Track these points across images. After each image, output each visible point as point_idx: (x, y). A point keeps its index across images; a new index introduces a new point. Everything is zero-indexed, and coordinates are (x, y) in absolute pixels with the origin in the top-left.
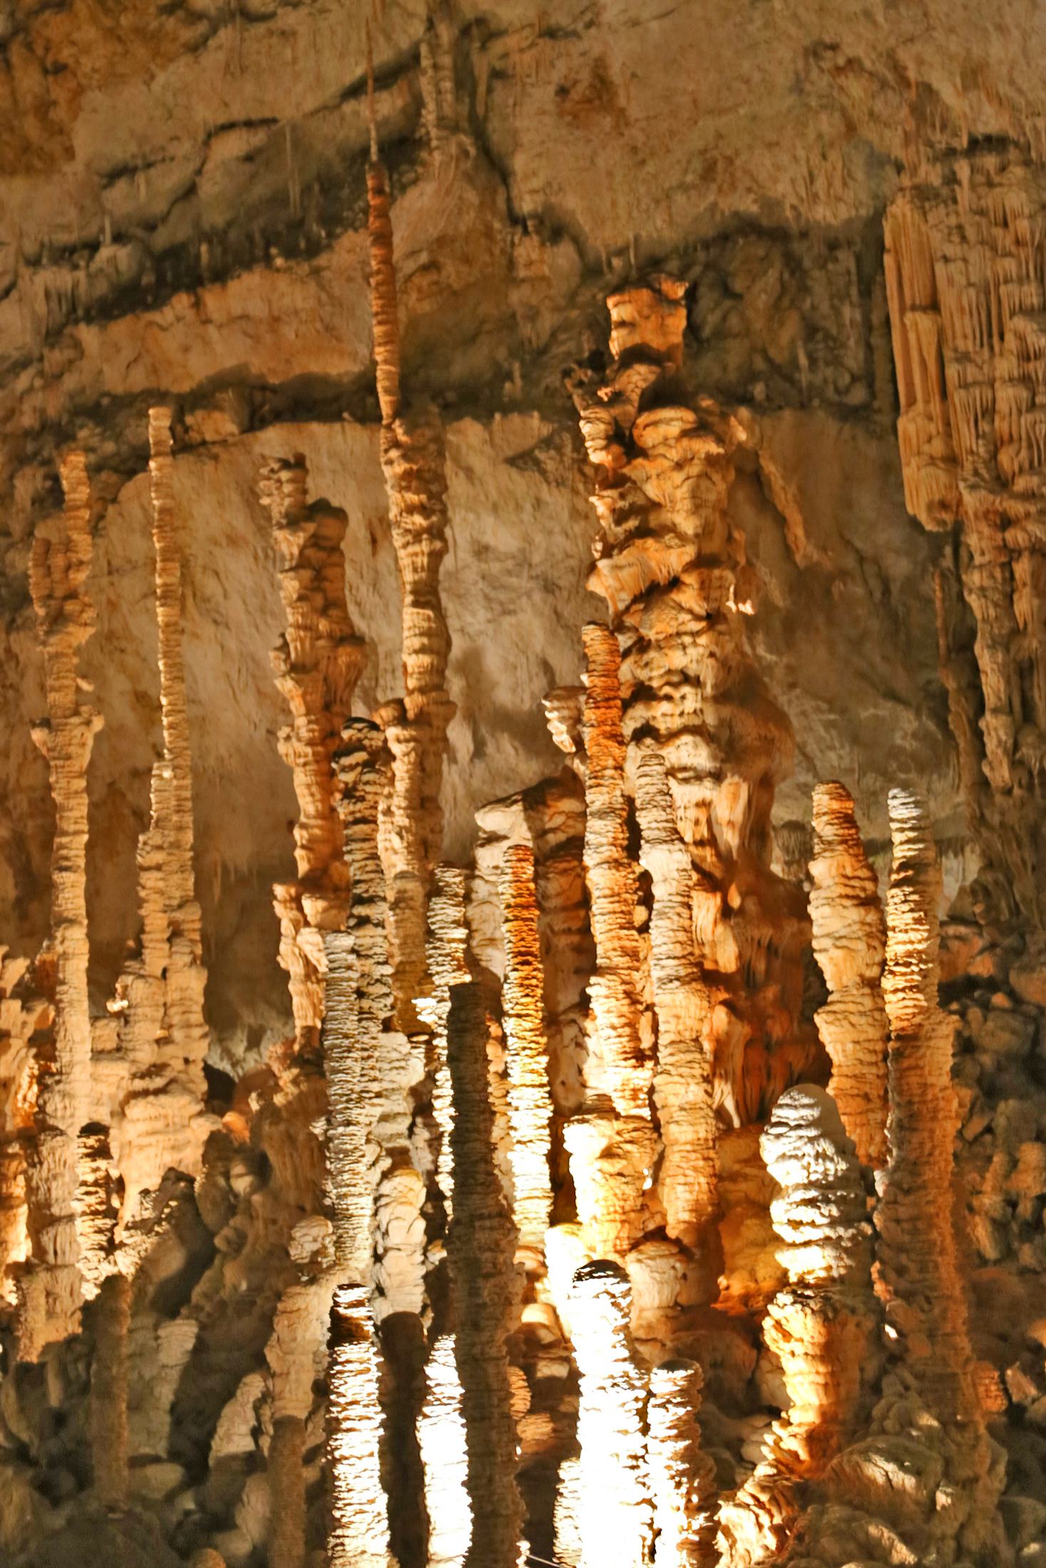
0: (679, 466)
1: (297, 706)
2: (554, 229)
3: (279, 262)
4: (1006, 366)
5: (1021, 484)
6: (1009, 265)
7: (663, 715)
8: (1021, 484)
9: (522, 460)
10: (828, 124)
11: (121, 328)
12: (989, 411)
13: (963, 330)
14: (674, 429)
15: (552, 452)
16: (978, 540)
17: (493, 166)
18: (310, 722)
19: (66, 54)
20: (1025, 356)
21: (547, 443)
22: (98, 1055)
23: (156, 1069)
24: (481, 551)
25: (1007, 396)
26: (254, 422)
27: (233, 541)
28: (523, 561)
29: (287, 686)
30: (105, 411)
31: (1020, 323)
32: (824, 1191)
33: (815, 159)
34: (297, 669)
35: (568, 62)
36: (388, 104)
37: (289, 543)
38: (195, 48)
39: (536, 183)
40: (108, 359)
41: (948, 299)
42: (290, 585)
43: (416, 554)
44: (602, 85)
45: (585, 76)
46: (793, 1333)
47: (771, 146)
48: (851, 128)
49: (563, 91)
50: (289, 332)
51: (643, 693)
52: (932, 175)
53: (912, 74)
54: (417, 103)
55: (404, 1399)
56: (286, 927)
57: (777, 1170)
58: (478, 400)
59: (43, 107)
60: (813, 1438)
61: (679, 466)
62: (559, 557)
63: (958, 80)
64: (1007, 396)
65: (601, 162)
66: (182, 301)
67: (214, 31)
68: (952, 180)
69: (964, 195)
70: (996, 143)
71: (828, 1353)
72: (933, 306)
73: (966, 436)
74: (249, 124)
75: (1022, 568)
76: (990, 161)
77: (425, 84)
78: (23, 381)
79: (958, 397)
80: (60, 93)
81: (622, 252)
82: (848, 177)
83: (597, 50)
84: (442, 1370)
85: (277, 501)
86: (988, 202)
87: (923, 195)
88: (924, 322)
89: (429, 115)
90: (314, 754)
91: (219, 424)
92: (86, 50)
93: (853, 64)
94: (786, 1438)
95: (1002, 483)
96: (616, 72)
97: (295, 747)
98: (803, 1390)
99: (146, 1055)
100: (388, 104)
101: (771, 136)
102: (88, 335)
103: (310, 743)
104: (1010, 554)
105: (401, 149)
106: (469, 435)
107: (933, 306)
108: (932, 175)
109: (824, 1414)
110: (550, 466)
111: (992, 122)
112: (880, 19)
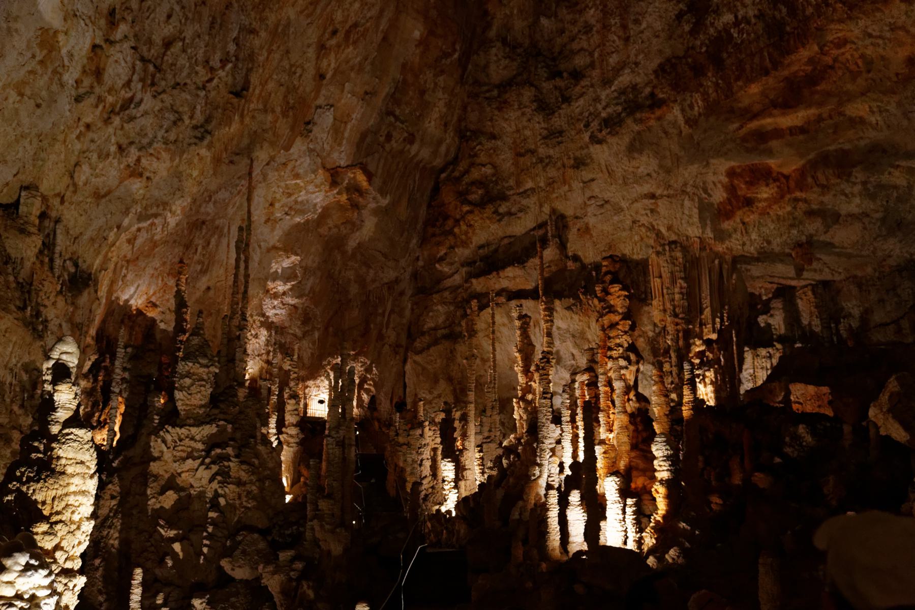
0: (618, 297)
1: (519, 359)
2: (576, 258)
4: (677, 290)
5: (680, 316)
6: (678, 268)
7: (614, 353)
8: (680, 316)
9: (568, 308)
10: (637, 238)
11: (481, 279)
12: (673, 300)
13: (667, 282)
14: (617, 289)
16: (670, 328)
17: (563, 246)
19: (472, 222)
20: (681, 288)
21: (574, 305)
22: (476, 433)
23: (488, 437)
24: (559, 328)
25: (677, 296)
26: (509, 299)
27: (504, 325)
28: (568, 331)
29: (517, 355)
30: (479, 296)
31: (680, 281)
32: (668, 458)
34: (519, 351)
35: (580, 224)
36: (541, 232)
37: (517, 323)
38: (499, 221)
40: (478, 285)
41: (664, 275)
42: (518, 332)
46: (660, 493)
48: (642, 239)
49: (579, 230)
50: (518, 280)
51: (610, 349)
52: (660, 249)
54: (547, 232)
55: (564, 503)
56: (516, 408)
57: (656, 453)
58: (560, 296)
59: (466, 233)
60: (664, 517)
61: (618, 297)
64: (677, 296)
66: (495, 273)
67: (503, 217)
68: (664, 250)
69: (667, 253)
70: (674, 242)
71: (668, 497)
72: (660, 277)
73: (668, 305)
74: (510, 237)
75: (681, 335)
76: (673, 246)
77: (549, 228)
78: (460, 290)
79: (666, 297)
80: (470, 231)
81: (591, 264)
82: (641, 249)
84: (575, 497)
85: (515, 314)
86: (673, 254)
87: (658, 253)
88: (658, 280)
89: (549, 234)
91: (502, 300)
92: (476, 221)
93: (643, 225)
94: (658, 517)
95: (676, 315)
96: (591, 226)
97: (518, 369)
98: (662, 505)
99: (486, 434)
100: (541, 232)
102: (474, 281)
104: (678, 331)
105: (544, 242)
106: (557, 303)
107: (660, 277)
108: (660, 249)
109: (667, 511)
111: (674, 237)
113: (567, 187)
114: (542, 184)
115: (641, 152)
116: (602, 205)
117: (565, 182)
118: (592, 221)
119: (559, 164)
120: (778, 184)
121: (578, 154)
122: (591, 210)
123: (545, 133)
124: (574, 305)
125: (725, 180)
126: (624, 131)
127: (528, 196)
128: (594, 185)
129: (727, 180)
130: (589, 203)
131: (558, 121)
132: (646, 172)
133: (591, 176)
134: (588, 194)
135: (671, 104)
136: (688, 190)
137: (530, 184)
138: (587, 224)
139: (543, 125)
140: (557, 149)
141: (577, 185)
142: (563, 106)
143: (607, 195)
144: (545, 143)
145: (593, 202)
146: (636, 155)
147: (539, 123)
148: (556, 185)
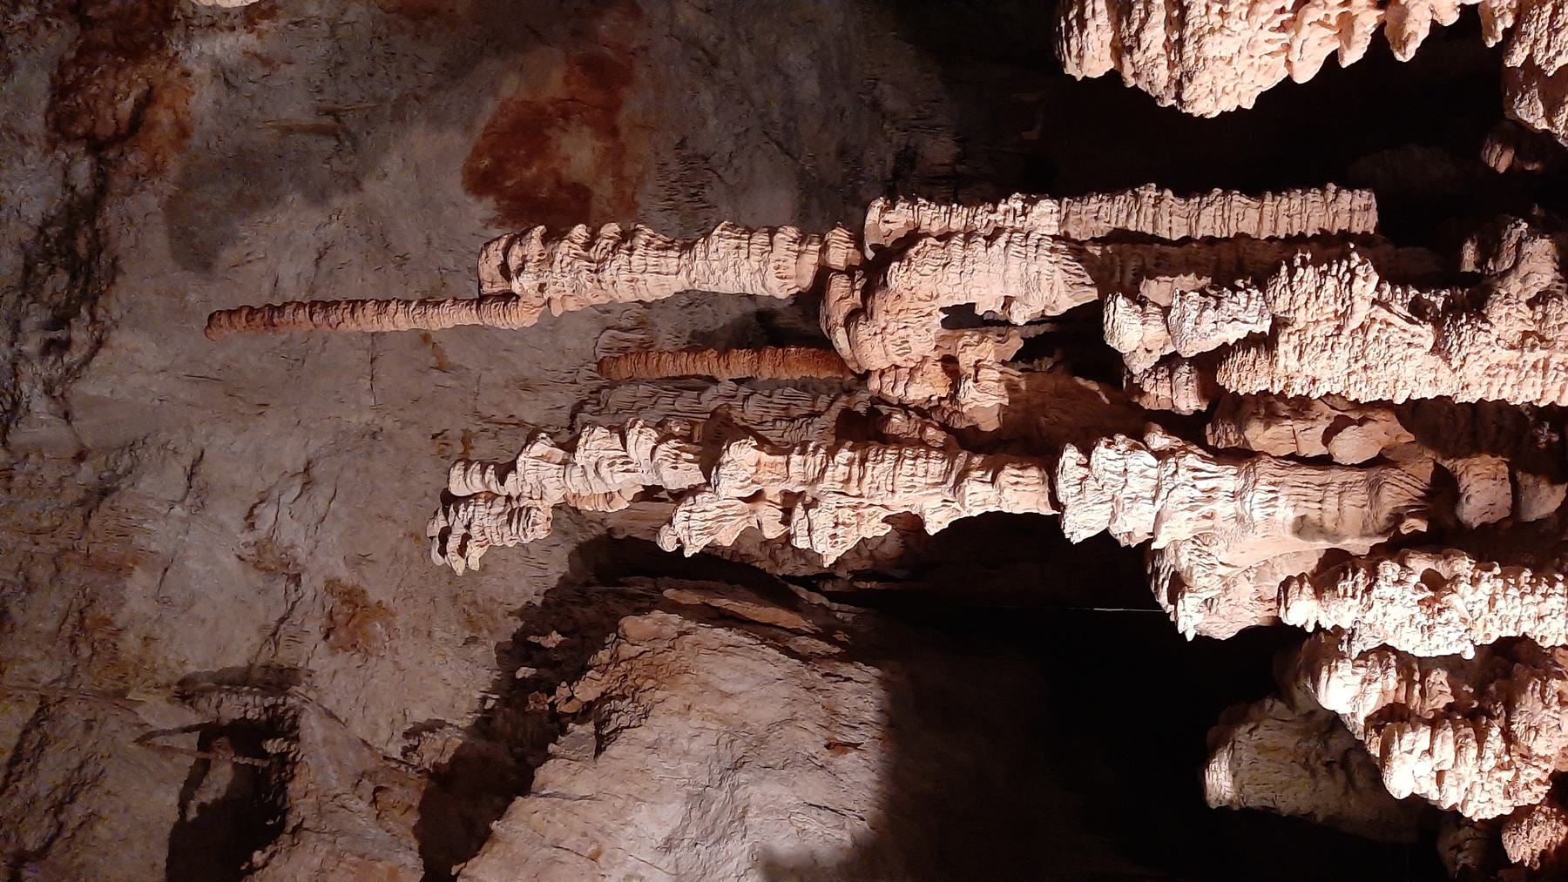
3: (258, 857)
15: (614, 716)
39: (384, 734)
43: (648, 244)
44: (352, 597)
45: (330, 602)
53: (500, 416)
62: (714, 751)
63: (524, 395)
65: (405, 663)
83: (319, 583)
90: (852, 449)
96: (346, 576)
110: (624, 721)
113: (139, 583)
114: (48, 672)
117: (119, 570)
118: (327, 562)
119: (41, 573)
121: (71, 494)
125: (484, 208)
126: (126, 243)
127: (41, 746)
128: (214, 470)
129: (490, 201)
130: (264, 527)
132: (306, 264)
133: (176, 472)
134: (230, 515)
135: (174, 75)
136: (449, 262)
138: (331, 585)
141: (159, 535)
143: (291, 454)
145: (267, 514)
146: (228, 255)
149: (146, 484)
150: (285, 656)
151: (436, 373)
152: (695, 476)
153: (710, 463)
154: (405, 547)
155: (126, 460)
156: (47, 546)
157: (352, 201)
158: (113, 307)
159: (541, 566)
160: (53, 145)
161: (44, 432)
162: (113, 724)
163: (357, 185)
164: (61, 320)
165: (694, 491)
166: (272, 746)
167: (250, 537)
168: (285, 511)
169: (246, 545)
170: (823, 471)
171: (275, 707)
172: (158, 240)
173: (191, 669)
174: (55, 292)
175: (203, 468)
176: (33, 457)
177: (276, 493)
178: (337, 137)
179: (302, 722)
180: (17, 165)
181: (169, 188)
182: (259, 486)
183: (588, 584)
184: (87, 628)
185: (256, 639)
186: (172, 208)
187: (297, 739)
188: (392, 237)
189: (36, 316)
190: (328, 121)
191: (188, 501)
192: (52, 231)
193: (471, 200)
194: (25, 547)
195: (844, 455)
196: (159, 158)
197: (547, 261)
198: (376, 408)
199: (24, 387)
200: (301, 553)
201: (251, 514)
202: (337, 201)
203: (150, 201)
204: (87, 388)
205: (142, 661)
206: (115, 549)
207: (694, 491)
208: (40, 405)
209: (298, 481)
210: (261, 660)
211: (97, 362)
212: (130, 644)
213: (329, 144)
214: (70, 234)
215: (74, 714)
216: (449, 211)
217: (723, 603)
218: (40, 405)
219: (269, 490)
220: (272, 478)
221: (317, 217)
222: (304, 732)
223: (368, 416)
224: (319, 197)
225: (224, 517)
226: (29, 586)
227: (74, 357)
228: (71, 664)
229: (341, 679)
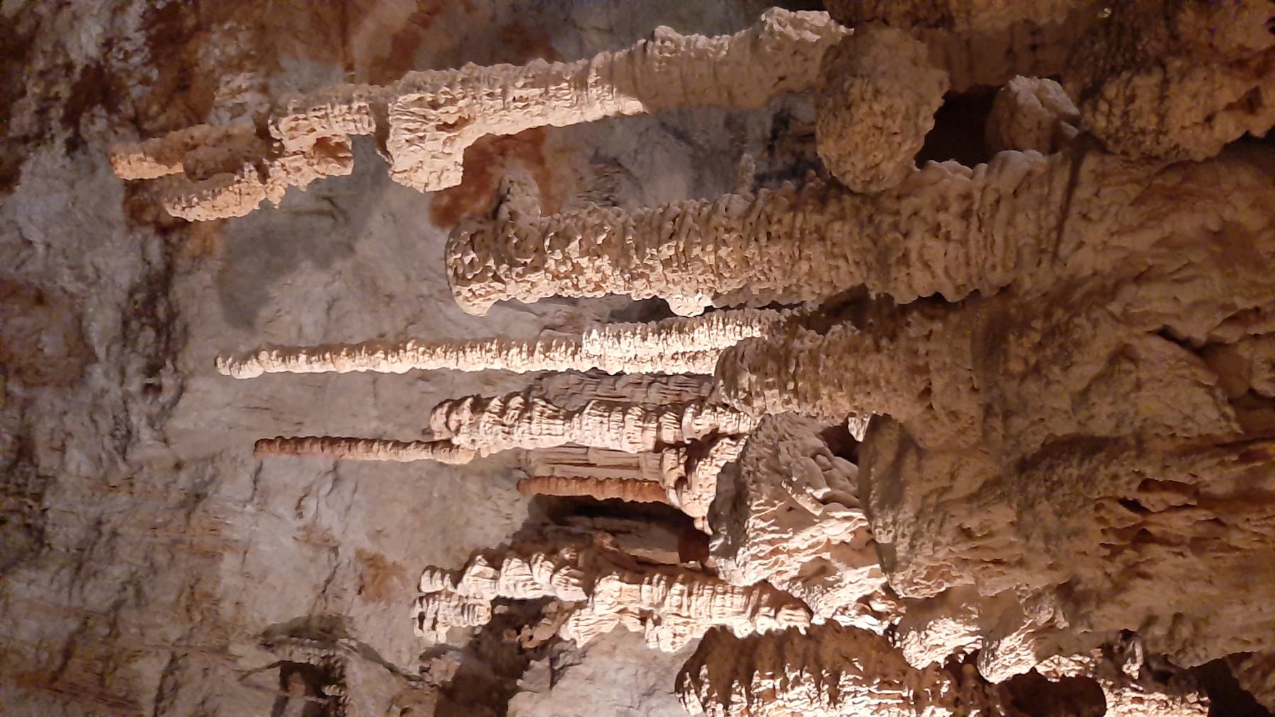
15: (562, 655)
18: (650, 583)
33: (489, 504)
39: (405, 658)
43: (542, 413)
44: (374, 562)
45: (361, 567)
47: (468, 523)
62: (633, 680)
83: (351, 553)
90: (683, 583)
96: (370, 547)
101: (462, 521)
103: (669, 586)
110: (569, 659)
112: (431, 389)
113: (229, 562)
114: (174, 632)
115: (264, 300)
116: (336, 481)
117: (213, 556)
119: (161, 558)
120: (511, 152)
121: (175, 497)
122: (330, 520)
123: (66, 575)
124: (553, 661)
126: (193, 310)
127: (176, 687)
130: (309, 516)
131: (65, 533)
132: (319, 313)
133: (245, 478)
134: (284, 507)
136: (424, 289)
137: (149, 671)
138: (359, 554)
139: (45, 577)
140: (124, 550)
141: (239, 526)
142: (46, 504)
144: (88, 578)
145: (310, 504)
146: (265, 313)
147: (31, 582)
148: (205, 587)
149: (226, 490)
150: (332, 608)
151: (421, 383)
152: (580, 595)
153: (590, 590)
154: (409, 519)
155: (210, 470)
156: (163, 537)
157: (349, 264)
158: (188, 359)
159: (508, 517)
160: (131, 229)
161: (149, 453)
162: (221, 671)
163: (351, 249)
164: (153, 369)
165: (580, 605)
166: (329, 691)
167: (300, 523)
168: (322, 503)
169: (299, 529)
170: (664, 599)
171: (327, 657)
172: (214, 308)
173: (270, 622)
174: (146, 346)
175: (263, 475)
176: (146, 469)
177: (314, 488)
178: (333, 217)
179: (348, 672)
180: (108, 244)
181: (218, 265)
182: (303, 484)
183: (544, 525)
184: (196, 599)
185: (312, 596)
186: (221, 281)
187: (344, 686)
188: (381, 283)
189: (136, 364)
190: (326, 206)
191: (256, 500)
192: (139, 297)
193: (437, 231)
194: (148, 539)
195: (678, 587)
196: (208, 243)
197: (474, 425)
198: (380, 418)
199: (134, 419)
200: (337, 532)
201: (298, 507)
202: (338, 264)
203: (205, 277)
204: (178, 423)
205: (236, 620)
206: (209, 542)
207: (580, 605)
208: (146, 434)
209: (330, 477)
210: (317, 612)
211: (182, 403)
212: (227, 609)
213: (326, 223)
214: (151, 301)
215: (194, 664)
216: (421, 245)
217: (640, 552)
218: (146, 434)
219: (310, 486)
220: (312, 477)
221: (324, 277)
222: (349, 680)
223: (374, 424)
224: (324, 263)
225: (281, 510)
226: (154, 569)
227: (165, 398)
228: (189, 626)
229: (373, 620)
